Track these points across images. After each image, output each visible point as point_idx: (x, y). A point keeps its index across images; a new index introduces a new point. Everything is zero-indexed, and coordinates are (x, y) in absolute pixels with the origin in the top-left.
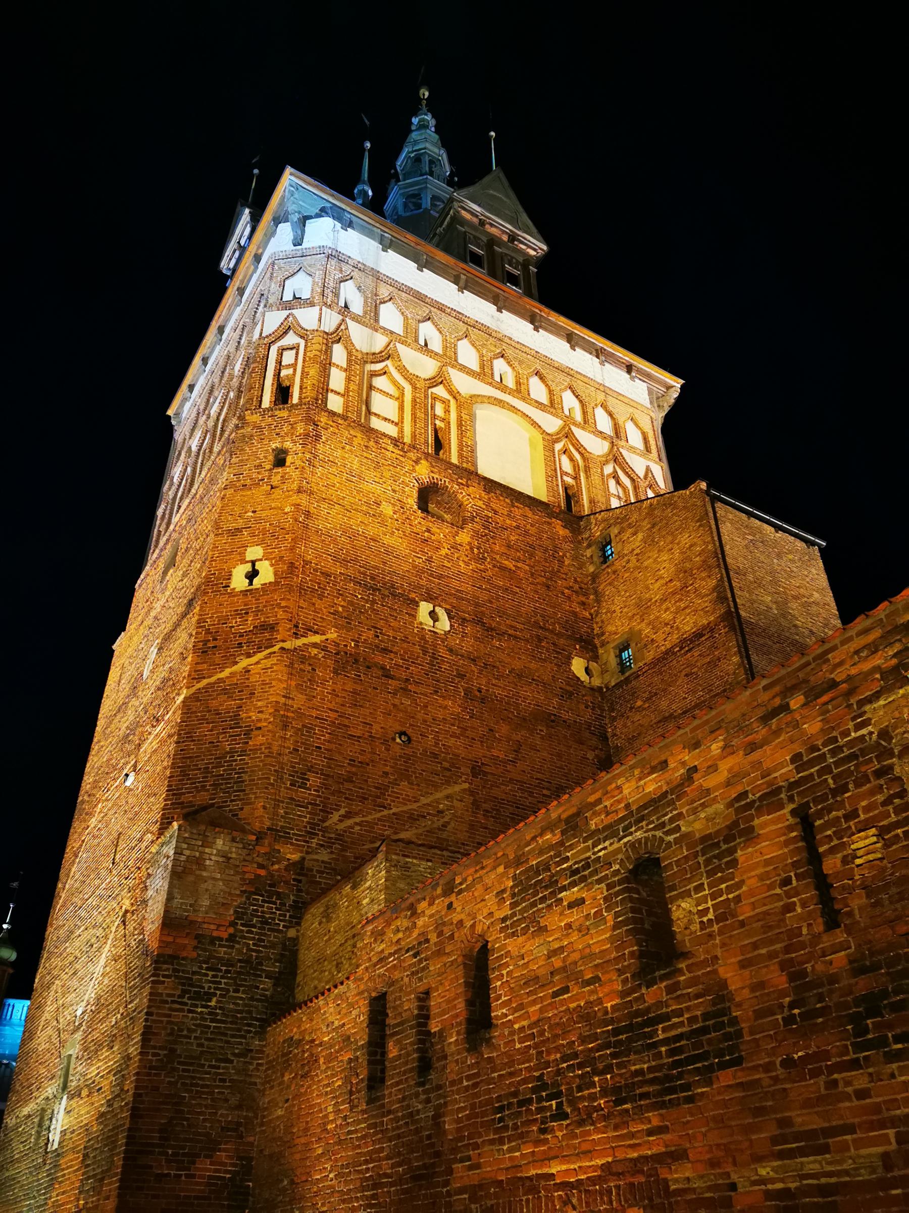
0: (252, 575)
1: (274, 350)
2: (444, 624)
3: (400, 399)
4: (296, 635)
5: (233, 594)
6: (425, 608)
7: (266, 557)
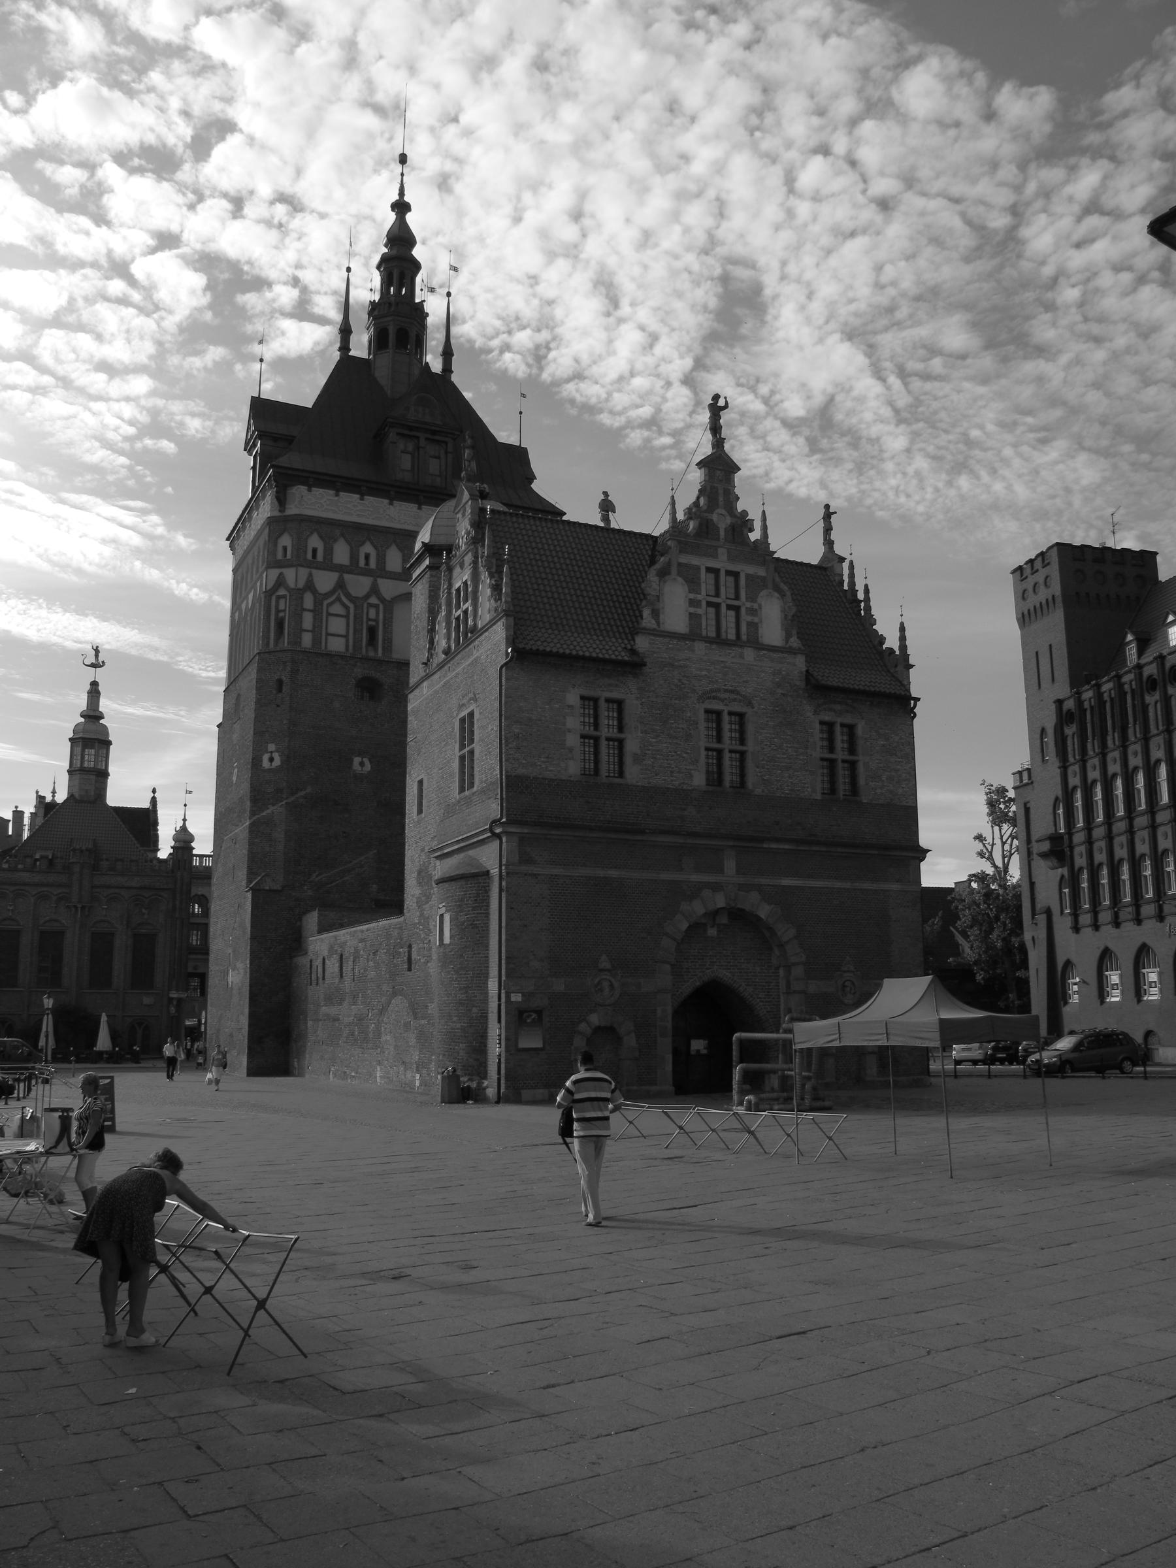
0: (271, 760)
1: (274, 598)
2: (368, 767)
3: (347, 617)
5: (265, 771)
6: (357, 760)
7: (277, 751)
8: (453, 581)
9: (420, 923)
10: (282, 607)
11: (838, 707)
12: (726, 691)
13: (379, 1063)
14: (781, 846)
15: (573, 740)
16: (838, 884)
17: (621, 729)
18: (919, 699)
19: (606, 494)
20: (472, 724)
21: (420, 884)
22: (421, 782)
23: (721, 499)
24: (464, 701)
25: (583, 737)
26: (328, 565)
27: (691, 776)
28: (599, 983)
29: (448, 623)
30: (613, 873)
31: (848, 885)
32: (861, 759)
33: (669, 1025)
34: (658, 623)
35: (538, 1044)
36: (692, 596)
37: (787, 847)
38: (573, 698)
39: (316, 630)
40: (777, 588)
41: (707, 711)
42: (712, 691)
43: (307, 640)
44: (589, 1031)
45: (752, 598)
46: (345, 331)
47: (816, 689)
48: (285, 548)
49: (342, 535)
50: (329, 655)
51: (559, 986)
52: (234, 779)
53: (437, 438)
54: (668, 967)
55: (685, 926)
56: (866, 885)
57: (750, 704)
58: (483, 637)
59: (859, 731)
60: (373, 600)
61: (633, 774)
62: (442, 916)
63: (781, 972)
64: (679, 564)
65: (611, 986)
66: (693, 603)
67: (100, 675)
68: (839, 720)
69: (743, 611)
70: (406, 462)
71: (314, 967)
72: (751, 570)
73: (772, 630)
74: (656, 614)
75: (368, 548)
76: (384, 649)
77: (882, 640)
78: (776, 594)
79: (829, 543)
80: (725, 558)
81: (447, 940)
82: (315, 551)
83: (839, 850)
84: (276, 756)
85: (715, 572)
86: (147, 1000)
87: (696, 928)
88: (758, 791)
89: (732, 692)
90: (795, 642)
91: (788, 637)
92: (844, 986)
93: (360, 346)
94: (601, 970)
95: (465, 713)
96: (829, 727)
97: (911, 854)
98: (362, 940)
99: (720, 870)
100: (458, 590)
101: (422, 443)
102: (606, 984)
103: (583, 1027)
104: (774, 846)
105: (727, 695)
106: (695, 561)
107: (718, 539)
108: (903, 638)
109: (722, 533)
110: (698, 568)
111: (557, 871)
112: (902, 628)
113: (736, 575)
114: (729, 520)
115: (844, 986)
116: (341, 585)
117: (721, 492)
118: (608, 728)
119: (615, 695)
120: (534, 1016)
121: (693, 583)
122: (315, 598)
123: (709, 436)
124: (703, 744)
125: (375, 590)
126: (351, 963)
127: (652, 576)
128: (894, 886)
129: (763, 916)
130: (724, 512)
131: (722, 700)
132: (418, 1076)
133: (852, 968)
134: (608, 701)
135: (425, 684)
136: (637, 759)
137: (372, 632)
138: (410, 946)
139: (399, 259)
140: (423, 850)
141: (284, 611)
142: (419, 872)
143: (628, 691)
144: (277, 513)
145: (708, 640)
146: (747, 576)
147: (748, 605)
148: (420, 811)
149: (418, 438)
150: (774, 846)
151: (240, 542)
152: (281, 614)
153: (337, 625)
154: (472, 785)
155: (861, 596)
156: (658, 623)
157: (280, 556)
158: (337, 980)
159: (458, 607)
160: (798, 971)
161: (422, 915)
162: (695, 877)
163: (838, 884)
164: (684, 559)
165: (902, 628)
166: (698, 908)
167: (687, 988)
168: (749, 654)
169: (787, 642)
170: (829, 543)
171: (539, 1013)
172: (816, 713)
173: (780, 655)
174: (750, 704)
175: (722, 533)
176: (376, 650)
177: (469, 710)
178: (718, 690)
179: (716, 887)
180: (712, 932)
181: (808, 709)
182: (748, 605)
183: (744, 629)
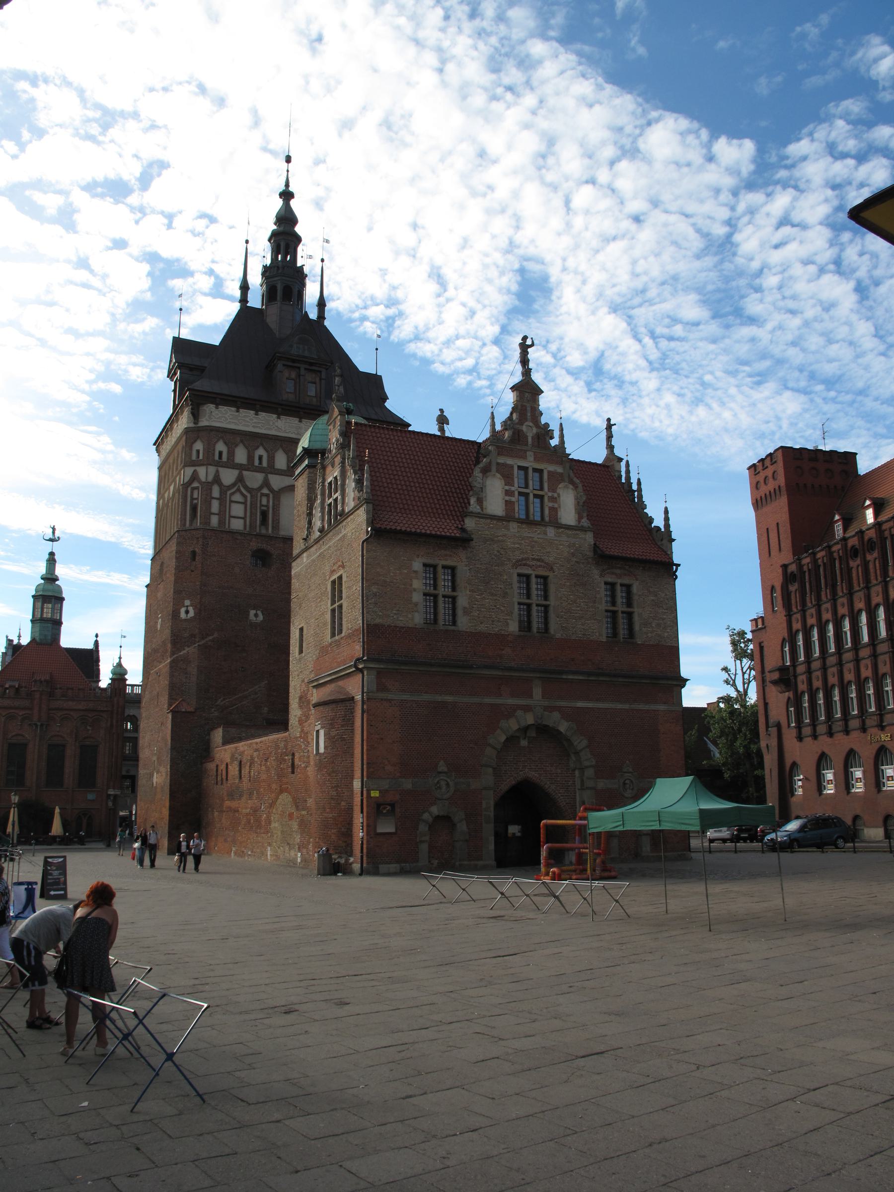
0: (187, 612)
1: (189, 489)
2: (261, 617)
3: (245, 503)
4: (203, 638)
6: (252, 612)
8: (326, 477)
9: (300, 737)
10: (195, 496)
11: (618, 571)
12: (533, 559)
13: (270, 844)
14: (576, 677)
15: (417, 597)
16: (620, 706)
17: (454, 589)
18: (679, 565)
19: (442, 411)
20: (341, 584)
21: (301, 707)
22: (301, 630)
23: (529, 414)
24: (335, 568)
25: (425, 594)
26: (231, 464)
27: (508, 624)
28: (438, 782)
29: (323, 508)
30: (449, 698)
31: (627, 706)
32: (636, 610)
33: (492, 814)
34: (482, 508)
35: (392, 829)
36: (507, 488)
37: (581, 678)
38: (417, 565)
39: (222, 513)
40: (572, 482)
41: (519, 575)
42: (523, 559)
43: (214, 520)
44: (431, 820)
45: (553, 489)
46: (245, 287)
47: (602, 558)
48: (198, 451)
49: (242, 441)
50: (232, 533)
51: (407, 784)
52: (159, 626)
53: (314, 368)
54: (490, 770)
55: (503, 738)
56: (641, 707)
57: (552, 569)
58: (349, 519)
59: (635, 589)
60: (265, 491)
61: (464, 623)
62: (318, 731)
63: (577, 773)
64: (498, 464)
65: (448, 785)
66: (508, 493)
67: (56, 547)
68: (619, 581)
69: (546, 499)
70: (290, 387)
71: (220, 771)
72: (552, 468)
73: (568, 514)
74: (480, 501)
75: (261, 451)
76: (273, 527)
77: (651, 520)
78: (571, 486)
79: (610, 447)
80: (532, 459)
81: (322, 750)
82: (221, 453)
83: (620, 680)
84: (191, 609)
85: (525, 469)
86: (91, 796)
87: (512, 740)
88: (558, 636)
89: (538, 560)
90: (585, 522)
91: (580, 518)
92: (624, 784)
93: (255, 300)
94: (440, 773)
95: (335, 577)
96: (612, 586)
97: (675, 683)
98: (257, 750)
99: (531, 696)
100: (330, 483)
101: (303, 372)
102: (443, 783)
103: (426, 816)
104: (570, 677)
105: (534, 563)
106: (509, 461)
107: (527, 445)
108: (667, 519)
109: (530, 440)
110: (512, 467)
111: (405, 697)
112: (666, 511)
113: (540, 471)
114: (535, 430)
115: (624, 784)
116: (240, 479)
117: (529, 409)
118: (444, 587)
119: (449, 563)
120: (389, 808)
121: (508, 478)
122: (221, 489)
123: (519, 368)
124: (516, 600)
125: (266, 483)
126: (247, 767)
127: (477, 472)
128: (662, 707)
129: (562, 730)
130: (531, 424)
131: (531, 566)
132: (299, 854)
133: (631, 770)
134: (444, 567)
135: (305, 555)
136: (466, 612)
137: (264, 514)
138: (293, 755)
139: (285, 236)
140: (303, 681)
141: (197, 499)
142: (301, 698)
143: (460, 560)
144: (192, 425)
145: (521, 522)
146: (549, 472)
147: (550, 494)
148: (301, 651)
149: (299, 368)
150: (570, 677)
151: (164, 446)
152: (195, 501)
153: (237, 510)
154: (340, 632)
155: (635, 487)
156: (482, 508)
157: (194, 457)
158: (237, 781)
159: (330, 496)
160: (590, 772)
161: (302, 731)
162: (511, 701)
163: (620, 706)
164: (501, 460)
165: (666, 511)
166: (513, 725)
167: (505, 787)
168: (551, 532)
169: (579, 522)
170: (610, 447)
171: (393, 805)
172: (601, 576)
173: (574, 532)
174: (552, 569)
175: (530, 440)
176: (267, 529)
177: (339, 574)
178: (527, 559)
179: (527, 709)
180: (524, 743)
181: (596, 573)
182: (550, 494)
183: (547, 512)
